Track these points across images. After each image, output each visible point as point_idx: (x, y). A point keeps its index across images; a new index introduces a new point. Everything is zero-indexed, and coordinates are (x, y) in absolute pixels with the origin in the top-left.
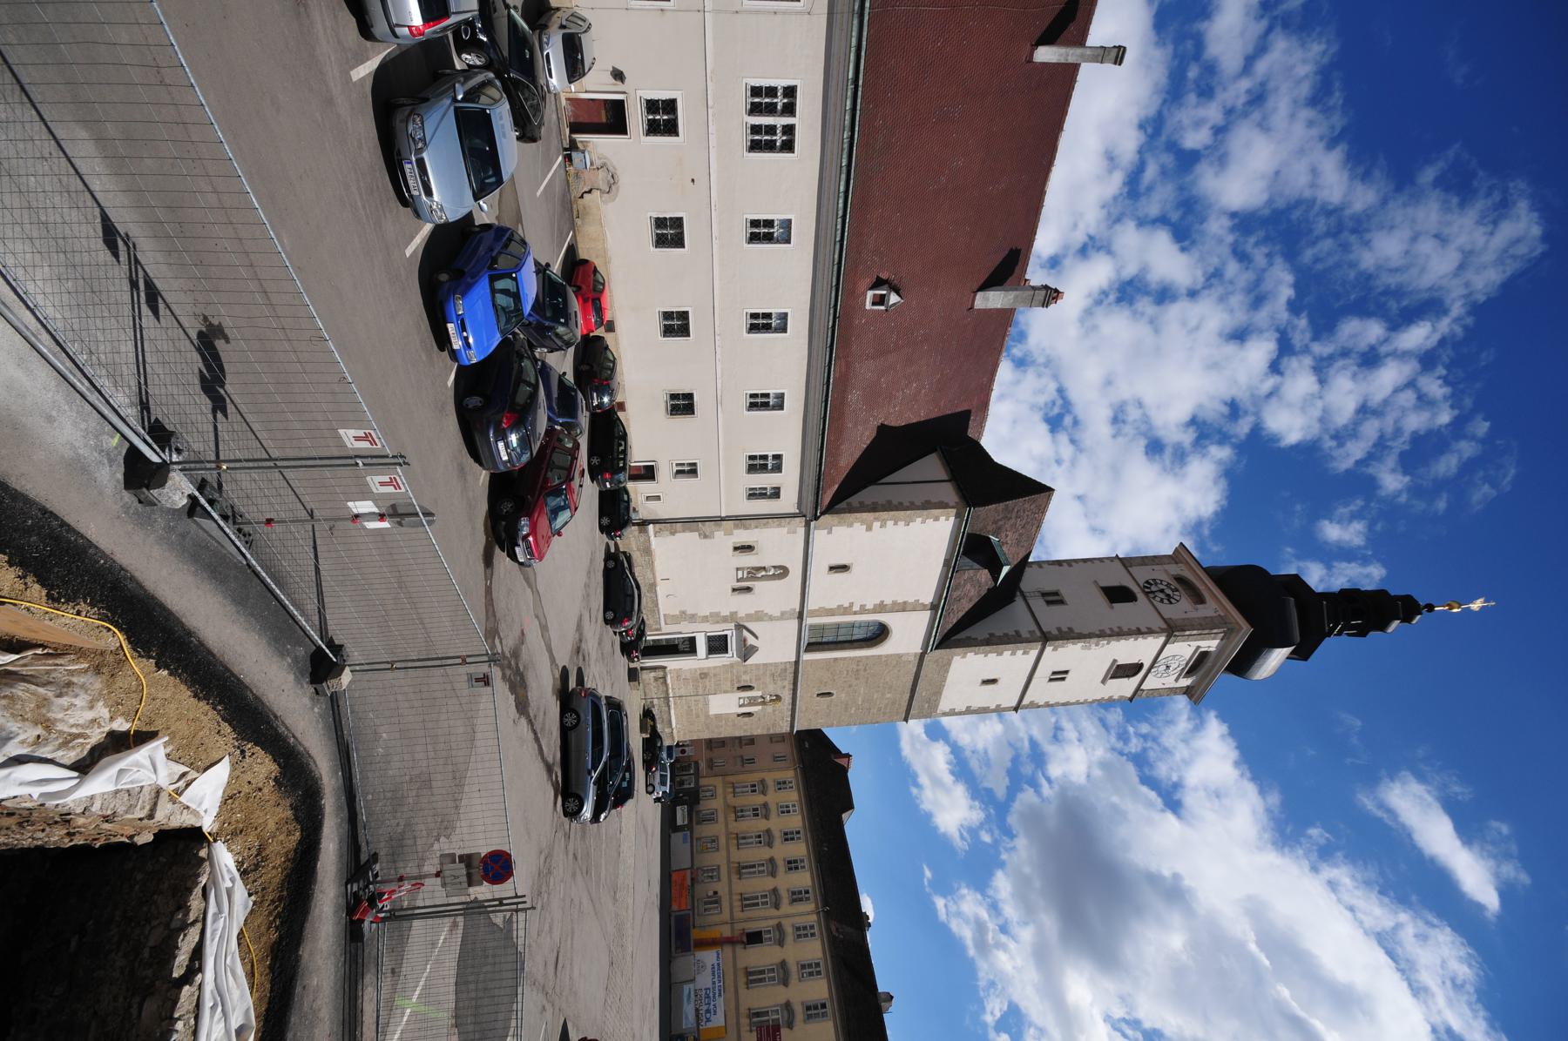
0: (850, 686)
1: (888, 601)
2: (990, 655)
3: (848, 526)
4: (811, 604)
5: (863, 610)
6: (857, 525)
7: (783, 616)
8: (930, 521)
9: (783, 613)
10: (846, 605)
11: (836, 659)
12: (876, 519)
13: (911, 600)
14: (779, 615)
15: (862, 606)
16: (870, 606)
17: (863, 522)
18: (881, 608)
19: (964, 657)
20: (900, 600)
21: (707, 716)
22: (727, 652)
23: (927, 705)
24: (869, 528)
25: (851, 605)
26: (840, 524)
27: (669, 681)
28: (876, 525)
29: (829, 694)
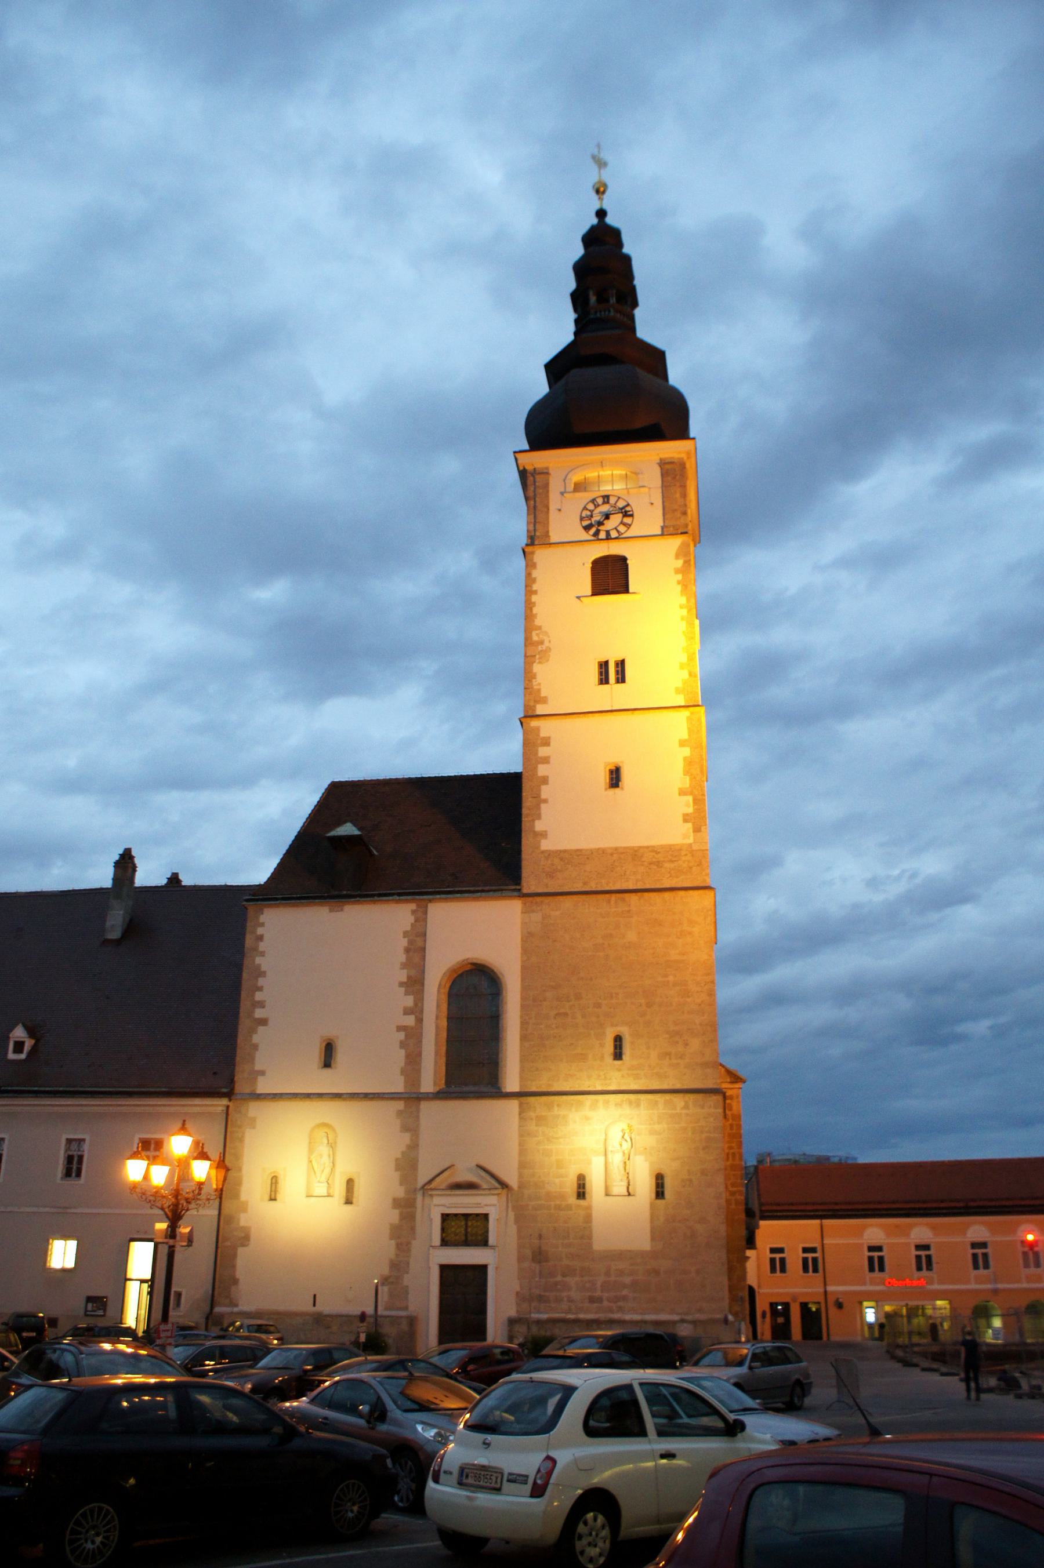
0: (598, 1005)
1: (403, 975)
2: (543, 796)
3: (257, 1050)
4: (399, 1087)
5: (416, 1010)
6: (256, 1039)
7: (411, 1127)
8: (262, 946)
9: (405, 1128)
10: (402, 1035)
11: (524, 1038)
12: (250, 1014)
13: (404, 942)
14: (406, 1138)
15: (407, 1012)
16: (409, 1001)
17: (253, 1031)
18: (415, 984)
19: (544, 835)
20: (403, 958)
21: (653, 1255)
22: (486, 1216)
23: (667, 865)
24: (264, 1022)
25: (400, 1028)
26: (252, 1059)
27: (544, 1316)
28: (259, 1013)
29: (618, 1040)
